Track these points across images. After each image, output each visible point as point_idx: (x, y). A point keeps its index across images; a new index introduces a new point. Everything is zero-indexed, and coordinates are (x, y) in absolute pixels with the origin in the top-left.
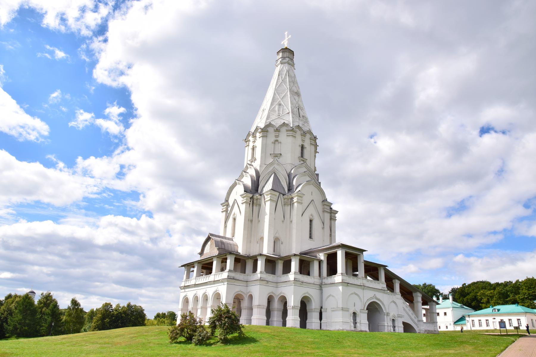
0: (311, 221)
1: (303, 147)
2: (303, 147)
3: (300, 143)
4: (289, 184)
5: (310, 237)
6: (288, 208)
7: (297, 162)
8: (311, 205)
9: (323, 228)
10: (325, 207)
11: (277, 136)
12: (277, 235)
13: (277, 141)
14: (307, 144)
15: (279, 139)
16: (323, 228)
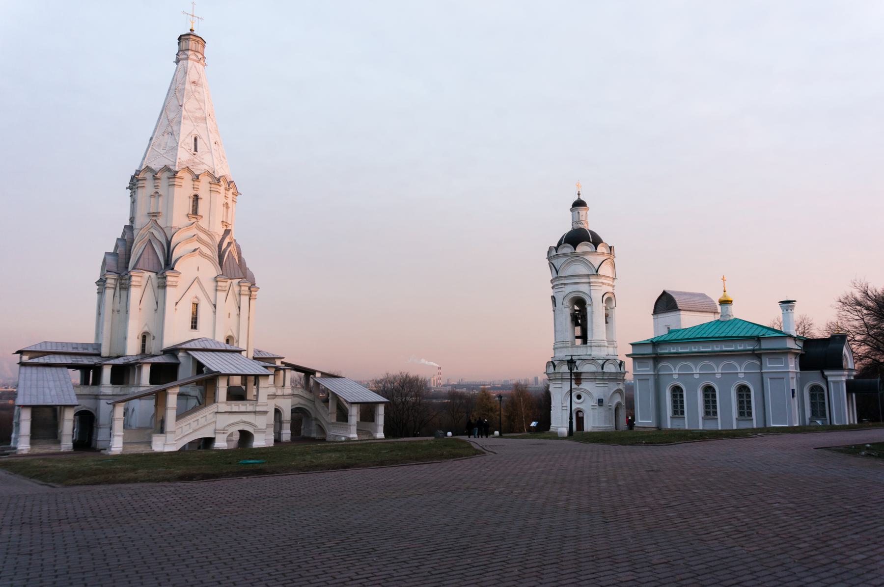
0: (196, 305)
1: (196, 198)
2: (196, 198)
4: (168, 256)
5: (194, 326)
6: (161, 291)
7: (187, 221)
8: (196, 284)
9: (215, 312)
10: (219, 284)
11: (156, 187)
12: (146, 329)
13: (157, 193)
14: (203, 192)
15: (160, 191)
16: (215, 312)
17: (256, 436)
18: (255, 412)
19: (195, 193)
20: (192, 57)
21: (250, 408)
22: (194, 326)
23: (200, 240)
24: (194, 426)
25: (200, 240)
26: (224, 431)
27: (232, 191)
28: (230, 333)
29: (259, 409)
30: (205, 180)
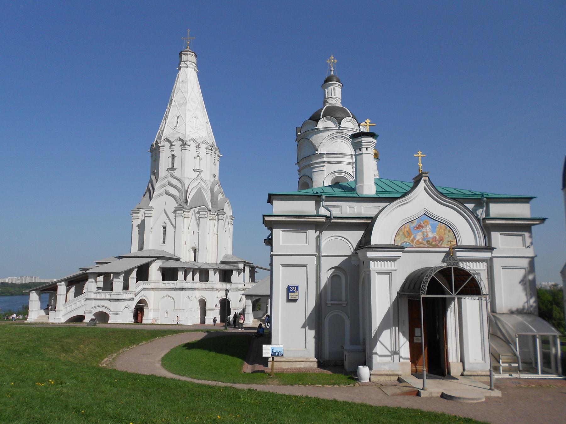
0: (164, 228)
3: (170, 154)
5: (164, 242)
17: (111, 316)
18: (109, 300)
19: (173, 153)
20: (191, 66)
21: (108, 296)
22: (164, 242)
23: (170, 184)
24: (73, 307)
25: (170, 184)
26: (90, 312)
27: (203, 146)
28: (194, 245)
29: (113, 297)
30: (178, 144)
